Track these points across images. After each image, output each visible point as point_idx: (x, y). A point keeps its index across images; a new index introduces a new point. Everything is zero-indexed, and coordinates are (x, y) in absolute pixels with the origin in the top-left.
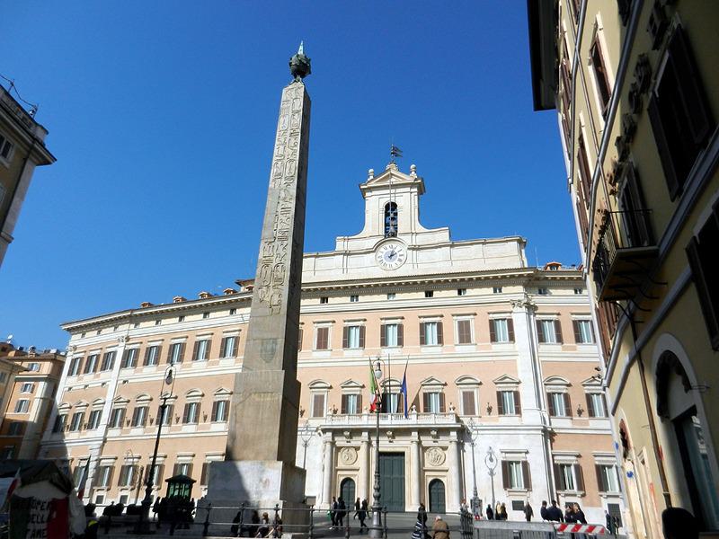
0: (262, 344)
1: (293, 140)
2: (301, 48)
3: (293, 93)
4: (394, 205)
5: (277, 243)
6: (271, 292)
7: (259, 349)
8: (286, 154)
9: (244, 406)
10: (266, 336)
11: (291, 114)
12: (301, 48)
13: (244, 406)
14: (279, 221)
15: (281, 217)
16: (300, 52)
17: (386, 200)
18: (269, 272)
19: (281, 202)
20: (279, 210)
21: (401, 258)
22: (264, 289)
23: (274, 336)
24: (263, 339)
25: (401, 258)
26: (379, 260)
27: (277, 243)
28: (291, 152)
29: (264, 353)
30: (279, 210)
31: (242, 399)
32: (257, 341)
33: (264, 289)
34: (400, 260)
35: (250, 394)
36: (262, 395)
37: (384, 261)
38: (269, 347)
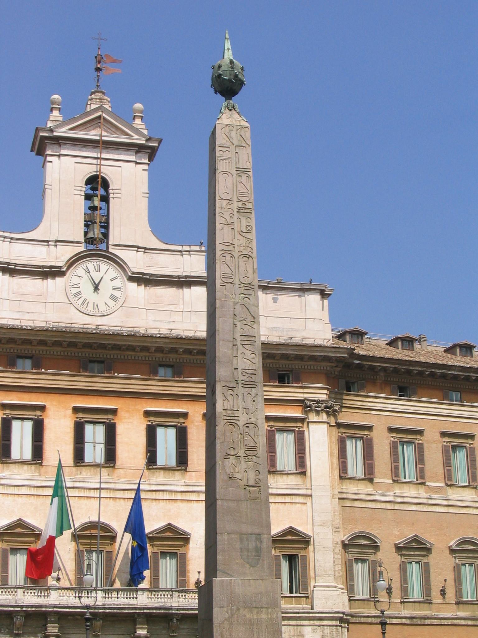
0: (241, 540)
1: (244, 222)
2: (228, 45)
3: (233, 134)
4: (105, 184)
5: (240, 390)
6: (243, 464)
7: (238, 546)
8: (236, 243)
9: (231, 624)
10: (246, 528)
11: (234, 172)
12: (228, 45)
13: (231, 624)
14: (240, 357)
15: (241, 349)
16: (229, 55)
17: (90, 170)
18: (235, 435)
19: (238, 324)
20: (239, 338)
21: (117, 294)
22: (232, 459)
23: (256, 530)
24: (241, 534)
25: (117, 294)
26: (75, 291)
27: (240, 390)
28: (243, 241)
29: (246, 553)
30: (237, 336)
31: (227, 615)
32: (233, 536)
33: (232, 459)
34: (114, 298)
35: (238, 609)
36: (255, 611)
37: (84, 296)
38: (252, 545)
